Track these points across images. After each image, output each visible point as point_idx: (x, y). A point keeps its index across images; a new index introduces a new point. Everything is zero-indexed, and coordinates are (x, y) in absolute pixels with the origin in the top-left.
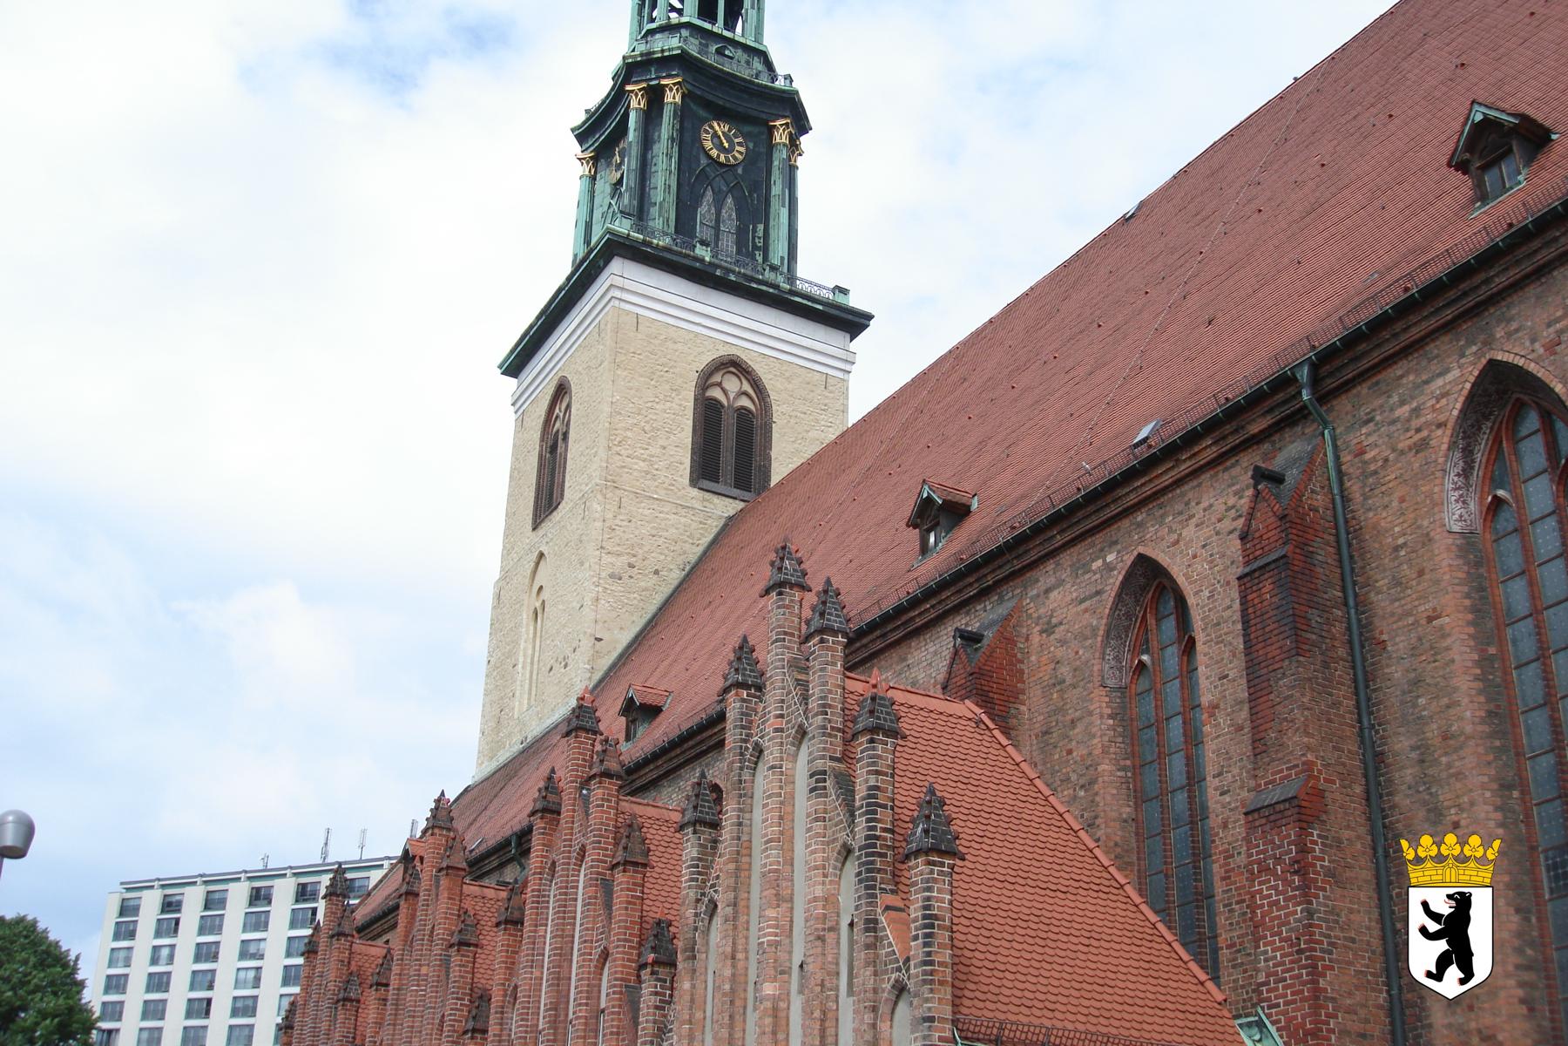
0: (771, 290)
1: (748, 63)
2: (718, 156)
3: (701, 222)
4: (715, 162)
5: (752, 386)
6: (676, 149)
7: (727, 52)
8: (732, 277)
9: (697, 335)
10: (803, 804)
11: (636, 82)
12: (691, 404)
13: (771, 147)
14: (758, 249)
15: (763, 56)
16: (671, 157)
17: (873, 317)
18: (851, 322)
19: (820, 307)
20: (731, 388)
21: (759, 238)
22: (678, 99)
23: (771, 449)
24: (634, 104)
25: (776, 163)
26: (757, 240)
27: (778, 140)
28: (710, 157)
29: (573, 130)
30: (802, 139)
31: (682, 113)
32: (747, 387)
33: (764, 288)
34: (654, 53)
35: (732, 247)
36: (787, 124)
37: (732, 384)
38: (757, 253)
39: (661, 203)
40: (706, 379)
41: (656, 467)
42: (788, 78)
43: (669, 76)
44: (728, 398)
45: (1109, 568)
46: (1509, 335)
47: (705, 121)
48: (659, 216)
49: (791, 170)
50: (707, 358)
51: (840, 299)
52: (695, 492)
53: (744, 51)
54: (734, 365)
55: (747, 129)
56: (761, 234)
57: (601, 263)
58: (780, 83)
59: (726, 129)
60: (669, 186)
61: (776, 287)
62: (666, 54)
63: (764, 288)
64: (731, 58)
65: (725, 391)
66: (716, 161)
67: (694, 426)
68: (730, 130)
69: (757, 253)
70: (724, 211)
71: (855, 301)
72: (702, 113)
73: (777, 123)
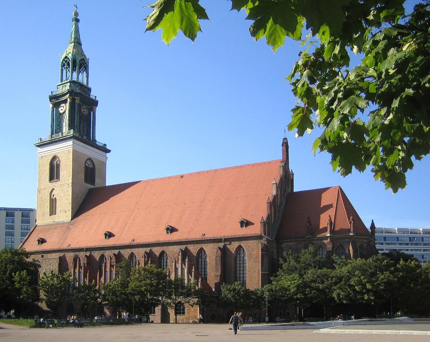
0: (96, 146)
4: (83, 114)
7: (85, 89)
15: (90, 90)
17: (111, 151)
19: (103, 149)
28: (83, 113)
31: (79, 104)
32: (91, 164)
33: (95, 146)
37: (89, 162)
46: (242, 243)
54: (90, 159)
55: (89, 107)
57: (69, 138)
59: (85, 107)
63: (95, 146)
71: (108, 147)
72: (81, 103)
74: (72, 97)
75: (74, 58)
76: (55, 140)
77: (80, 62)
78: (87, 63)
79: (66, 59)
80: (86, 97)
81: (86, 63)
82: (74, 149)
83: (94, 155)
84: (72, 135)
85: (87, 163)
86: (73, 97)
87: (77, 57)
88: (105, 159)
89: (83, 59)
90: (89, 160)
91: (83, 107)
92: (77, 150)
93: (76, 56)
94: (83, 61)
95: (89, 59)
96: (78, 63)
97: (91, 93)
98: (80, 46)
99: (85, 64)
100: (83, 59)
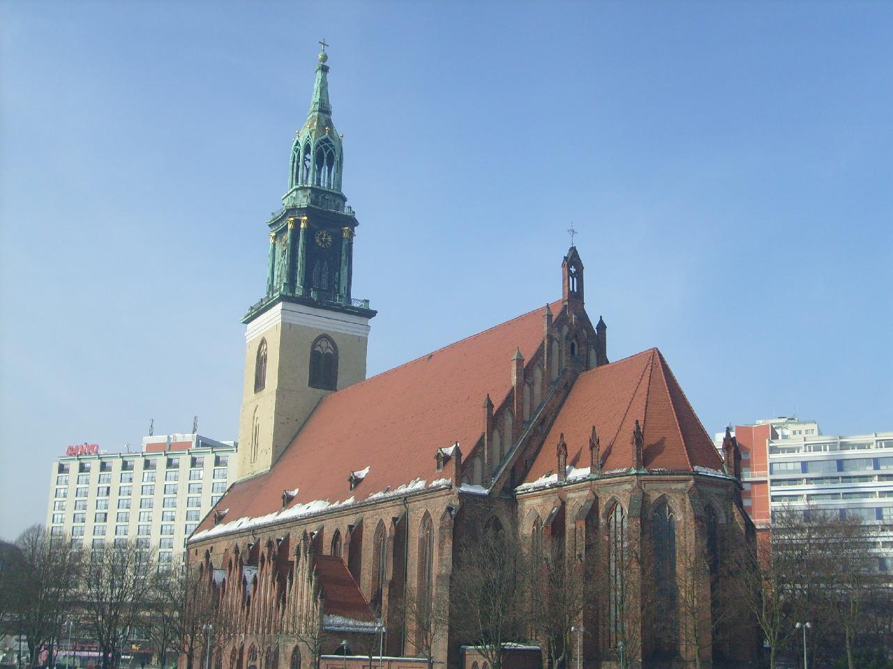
0: (339, 308)
8: (325, 305)
10: (306, 584)
11: (290, 217)
13: (342, 239)
14: (335, 283)
18: (370, 314)
20: (324, 347)
24: (290, 226)
31: (307, 231)
32: (330, 345)
37: (324, 344)
40: (314, 345)
43: (304, 216)
45: (377, 519)
50: (315, 337)
52: (310, 388)
54: (325, 337)
55: (333, 230)
56: (337, 276)
62: (302, 207)
71: (372, 307)
72: (316, 227)
81: (332, 146)
82: (286, 321)
88: (365, 332)
97: (344, 199)
98: (326, 116)
100: (327, 140)
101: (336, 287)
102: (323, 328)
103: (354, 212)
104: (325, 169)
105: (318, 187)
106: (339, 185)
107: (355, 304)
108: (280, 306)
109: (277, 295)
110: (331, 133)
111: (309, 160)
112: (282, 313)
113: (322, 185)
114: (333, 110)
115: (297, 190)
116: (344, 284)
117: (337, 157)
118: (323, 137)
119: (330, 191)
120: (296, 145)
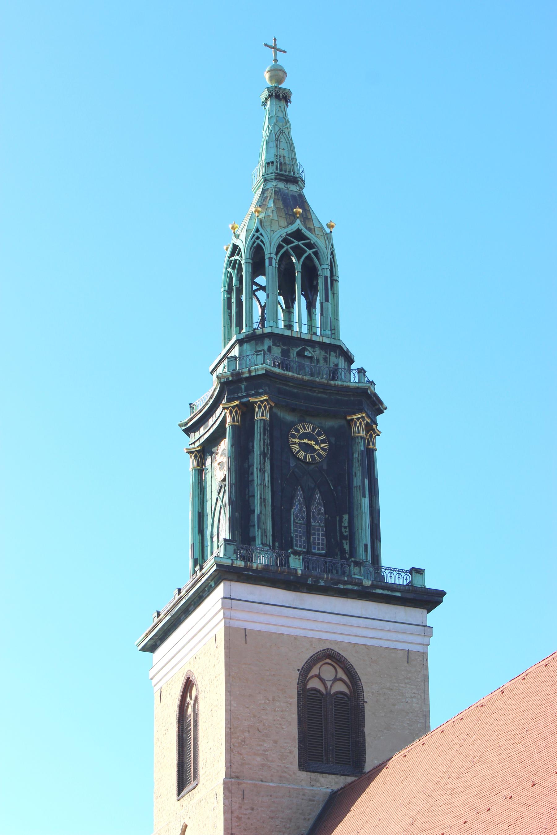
0: (356, 588)
1: (326, 359)
2: (305, 457)
3: (294, 522)
5: (345, 673)
6: (268, 462)
7: (306, 354)
8: (322, 583)
9: (296, 638)
12: (295, 700)
14: (345, 538)
16: (264, 472)
21: (345, 528)
22: (267, 417)
23: (364, 726)
25: (356, 455)
26: (343, 530)
27: (356, 434)
29: (180, 426)
30: (379, 418)
32: (341, 674)
33: (350, 587)
34: (242, 373)
35: (323, 540)
36: (363, 417)
38: (344, 542)
39: (258, 516)
41: (271, 759)
42: (361, 371)
43: (258, 394)
44: (326, 688)
47: (292, 425)
48: (258, 528)
49: (370, 453)
50: (307, 656)
51: (417, 583)
52: (304, 775)
53: (321, 349)
55: (330, 423)
56: (346, 523)
58: (354, 378)
59: (310, 430)
60: (265, 499)
61: (359, 583)
62: (253, 374)
63: (350, 587)
64: (311, 358)
65: (322, 681)
66: (304, 462)
67: (299, 719)
68: (314, 430)
69: (344, 542)
70: (314, 507)
72: (288, 417)
73: (355, 417)
74: (236, 403)
75: (254, 242)
76: (180, 605)
77: (283, 247)
78: (321, 243)
79: (233, 258)
80: (302, 384)
81: (310, 246)
83: (355, 631)
84: (215, 568)
85: (316, 680)
86: (244, 400)
87: (263, 234)
88: (419, 639)
89: (298, 231)
90: (328, 661)
91: (297, 431)
92: (249, 626)
93: (261, 231)
94: (296, 243)
95: (330, 226)
96: (273, 256)
97: (350, 360)
98: (293, 188)
99: (309, 252)
100: (298, 235)
101: (347, 547)
102: (325, 636)
103: (372, 383)
104: (300, 303)
105: (288, 333)
106: (334, 330)
107: (390, 579)
108: (219, 591)
109: (210, 566)
110: (307, 216)
111: (263, 288)
112: (223, 607)
113: (296, 328)
114: (307, 177)
115: (240, 342)
116: (365, 537)
117: (324, 271)
118: (293, 228)
119: (314, 338)
120: (232, 255)
